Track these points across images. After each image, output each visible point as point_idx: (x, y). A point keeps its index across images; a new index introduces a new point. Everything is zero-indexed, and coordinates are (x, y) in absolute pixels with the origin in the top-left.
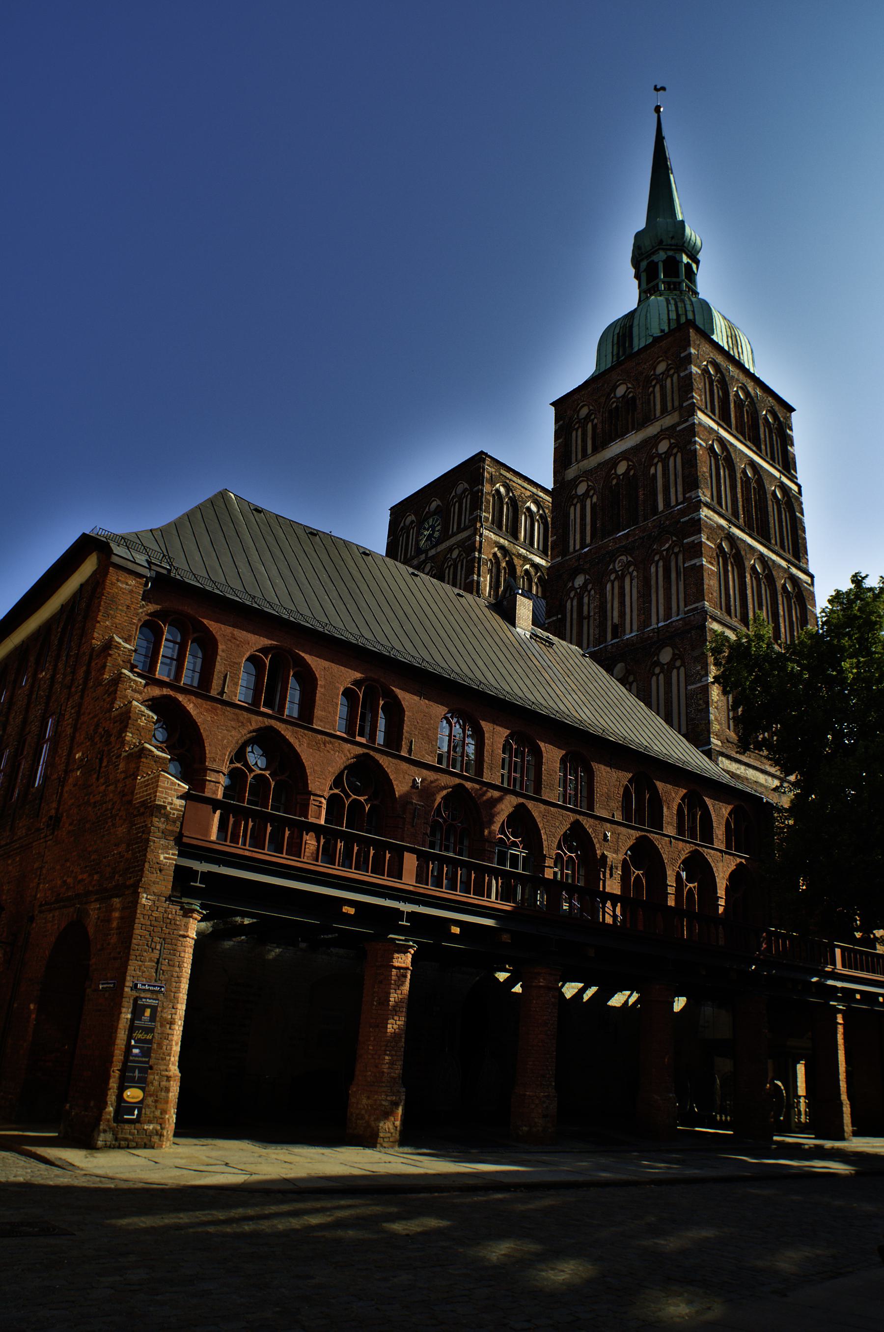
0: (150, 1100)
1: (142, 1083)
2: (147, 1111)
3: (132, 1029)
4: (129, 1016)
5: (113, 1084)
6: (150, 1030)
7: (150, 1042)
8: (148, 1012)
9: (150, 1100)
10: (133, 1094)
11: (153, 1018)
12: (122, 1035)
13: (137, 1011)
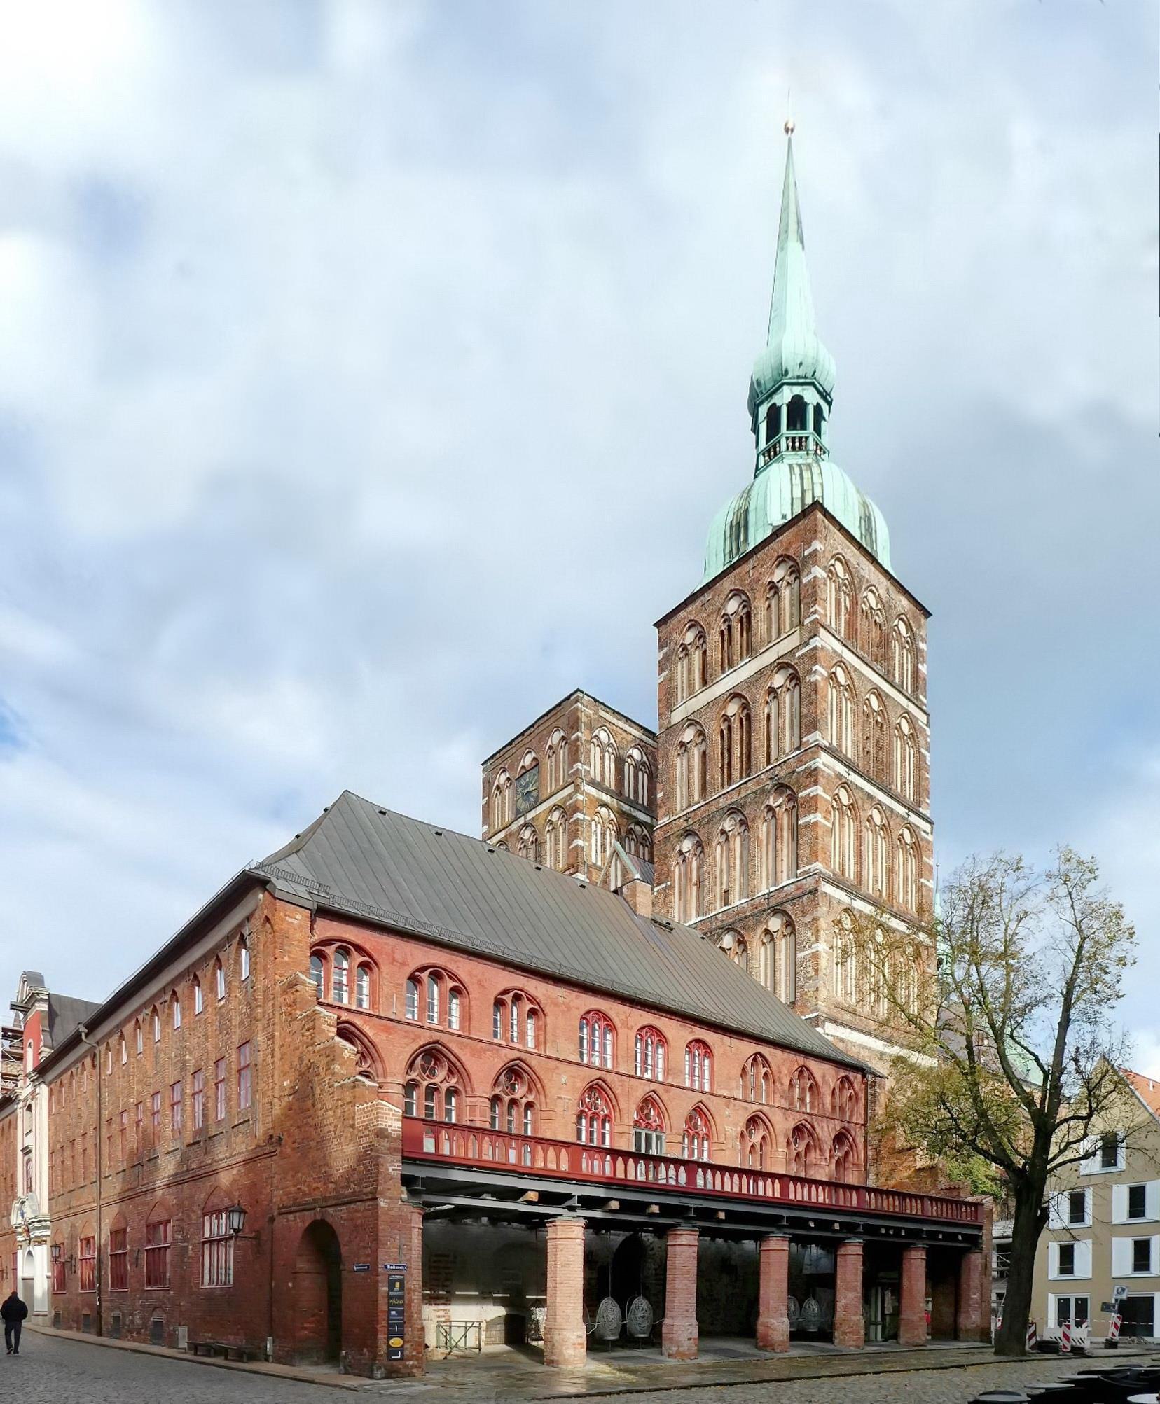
0: (407, 1346)
1: (401, 1334)
2: (407, 1353)
3: (390, 1297)
4: (386, 1289)
5: (381, 1338)
6: (401, 1297)
7: (402, 1305)
8: (398, 1285)
9: (407, 1346)
10: (396, 1342)
11: (402, 1288)
12: (382, 1304)
13: (391, 1285)
